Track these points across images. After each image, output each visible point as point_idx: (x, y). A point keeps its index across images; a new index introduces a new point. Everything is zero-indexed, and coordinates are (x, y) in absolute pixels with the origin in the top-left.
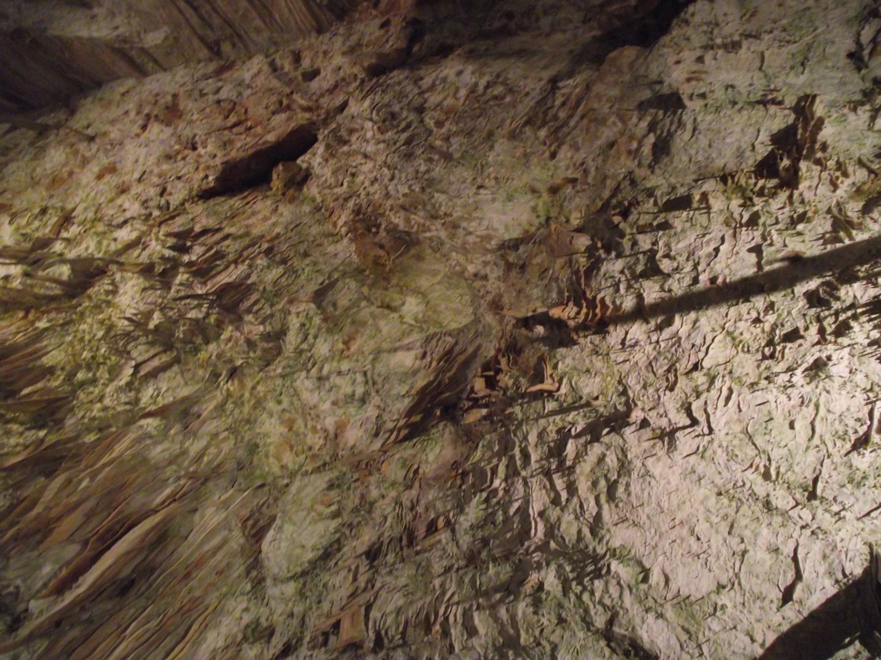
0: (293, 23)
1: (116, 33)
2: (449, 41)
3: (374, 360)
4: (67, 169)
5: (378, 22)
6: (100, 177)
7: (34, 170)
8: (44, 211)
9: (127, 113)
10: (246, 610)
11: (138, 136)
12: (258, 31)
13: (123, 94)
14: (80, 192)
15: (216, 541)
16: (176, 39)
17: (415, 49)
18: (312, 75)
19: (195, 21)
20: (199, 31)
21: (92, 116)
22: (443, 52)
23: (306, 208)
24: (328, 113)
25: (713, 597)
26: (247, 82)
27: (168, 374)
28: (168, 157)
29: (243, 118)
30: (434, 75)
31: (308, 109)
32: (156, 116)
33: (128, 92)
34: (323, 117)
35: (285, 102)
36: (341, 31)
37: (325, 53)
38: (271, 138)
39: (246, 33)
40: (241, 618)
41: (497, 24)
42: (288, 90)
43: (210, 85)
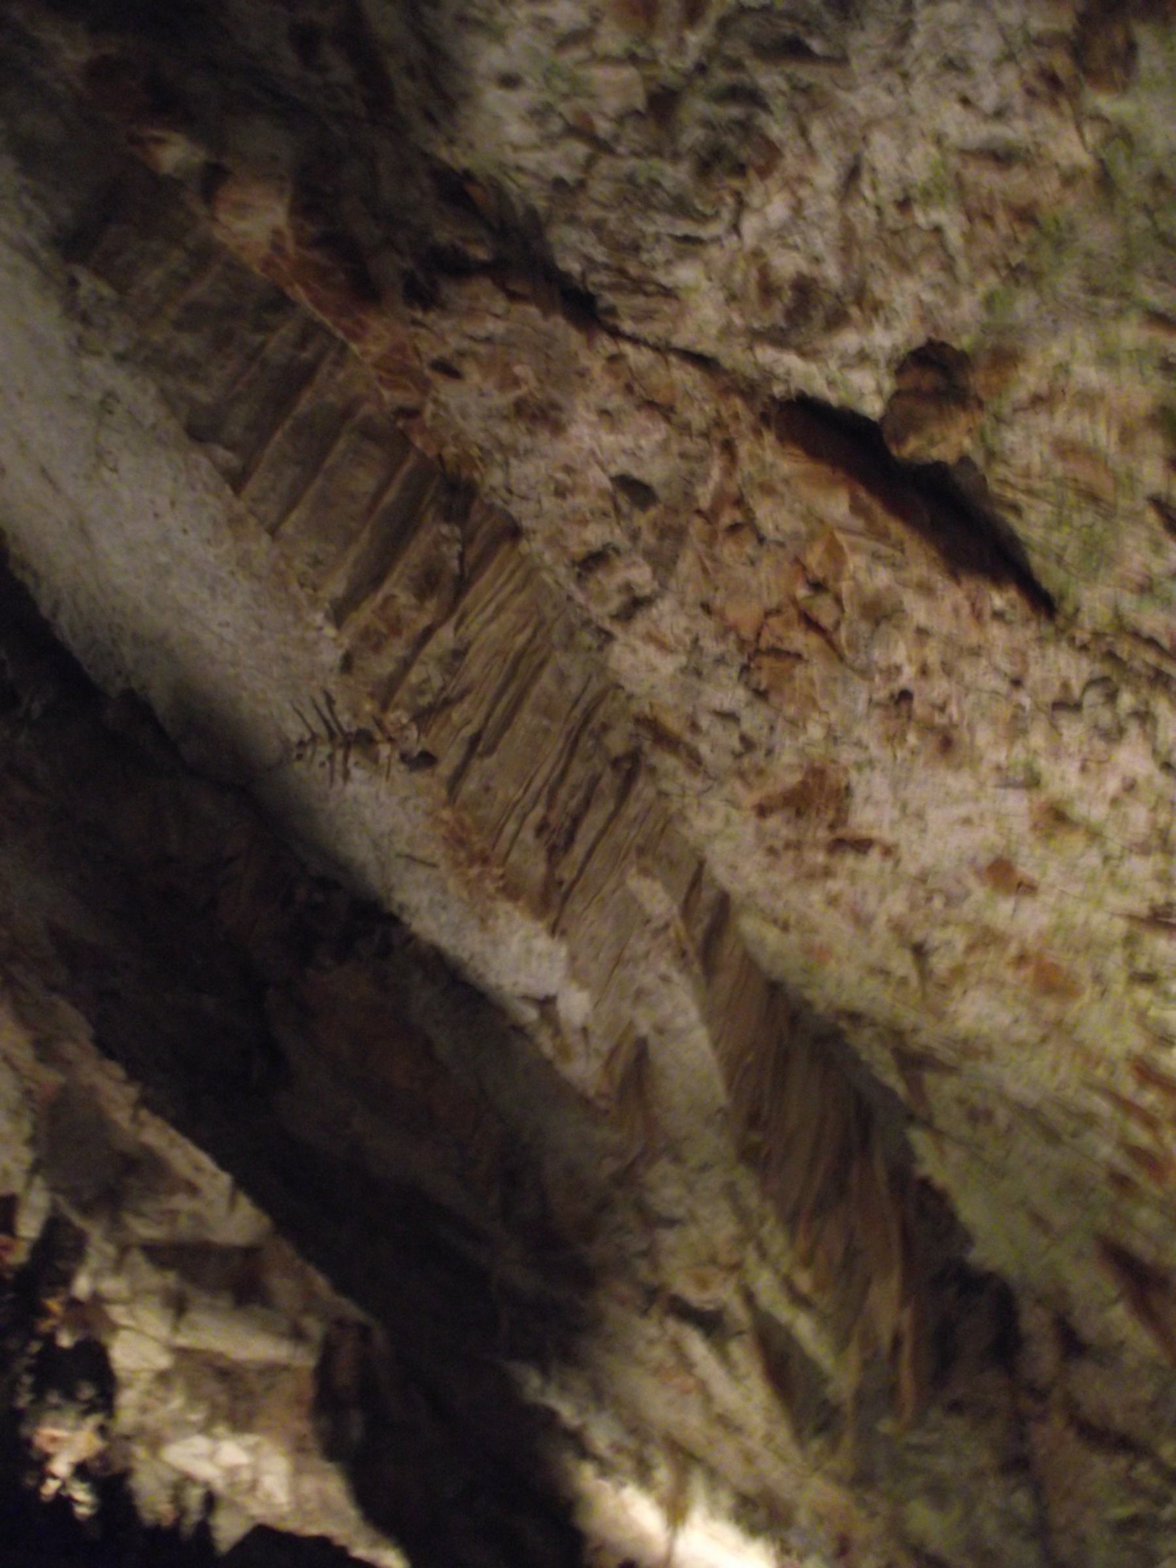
0: (521, 599)
1: (676, 976)
2: (426, 182)
4: (1009, 975)
5: (447, 391)
6: (1027, 888)
7: (1020, 1045)
8: (1148, 979)
9: (833, 901)
11: (888, 851)
12: (562, 678)
13: (785, 928)
14: (1079, 919)
16: (641, 851)
17: (481, 254)
18: (635, 490)
19: (595, 819)
20: (610, 806)
21: (851, 973)
22: (456, 189)
23: (1024, 305)
24: (725, 392)
26: (682, 659)
28: (947, 744)
29: (792, 612)
30: (530, 160)
31: (728, 447)
32: (832, 827)
33: (775, 922)
34: (738, 403)
35: (728, 517)
36: (496, 477)
37: (561, 492)
38: (837, 506)
39: (576, 703)
41: (341, 71)
42: (697, 526)
43: (713, 747)
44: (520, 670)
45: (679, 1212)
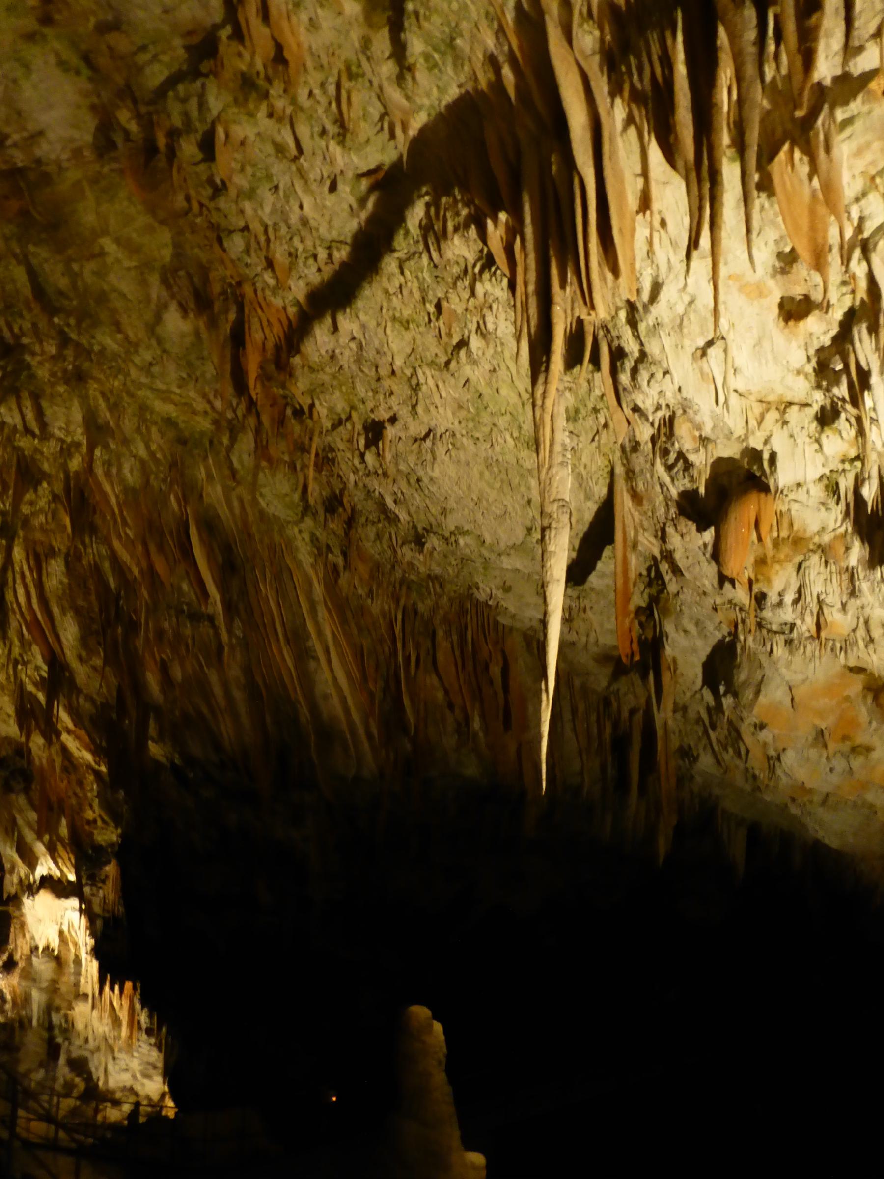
3: (159, 341)
10: (300, 531)
15: (236, 504)
25: (529, 539)
27: (48, 412)
40: (303, 539)
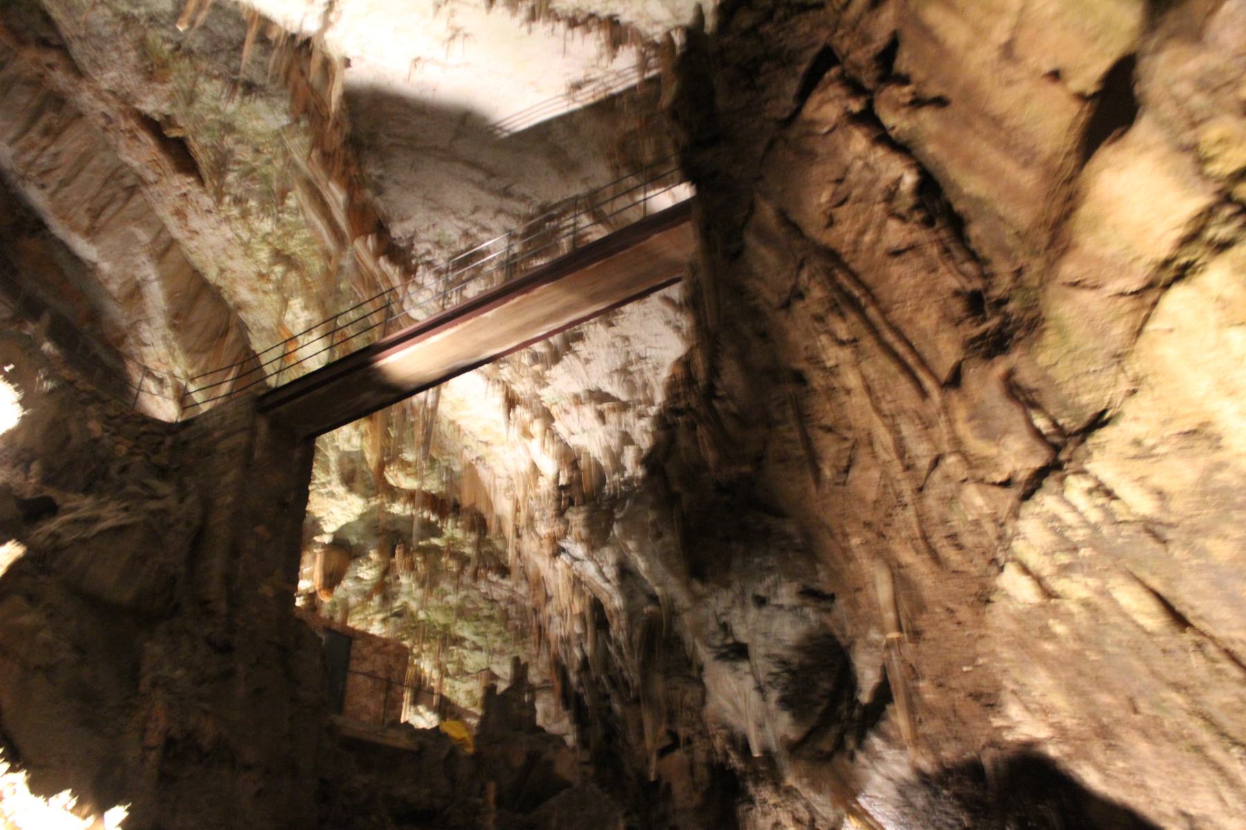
12: (103, 160)
44: (83, 159)
45: (148, 342)
